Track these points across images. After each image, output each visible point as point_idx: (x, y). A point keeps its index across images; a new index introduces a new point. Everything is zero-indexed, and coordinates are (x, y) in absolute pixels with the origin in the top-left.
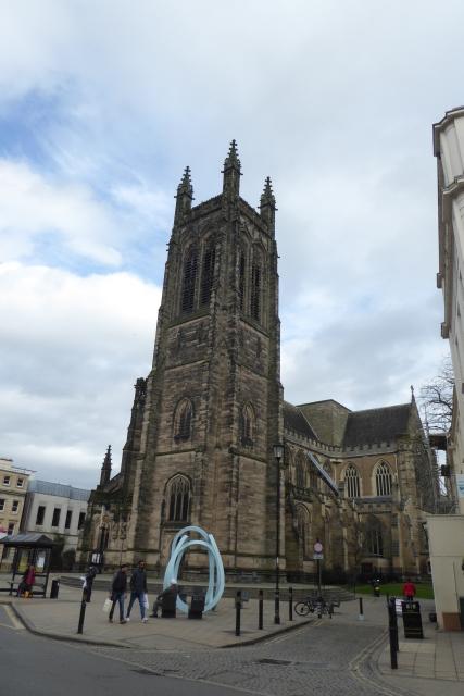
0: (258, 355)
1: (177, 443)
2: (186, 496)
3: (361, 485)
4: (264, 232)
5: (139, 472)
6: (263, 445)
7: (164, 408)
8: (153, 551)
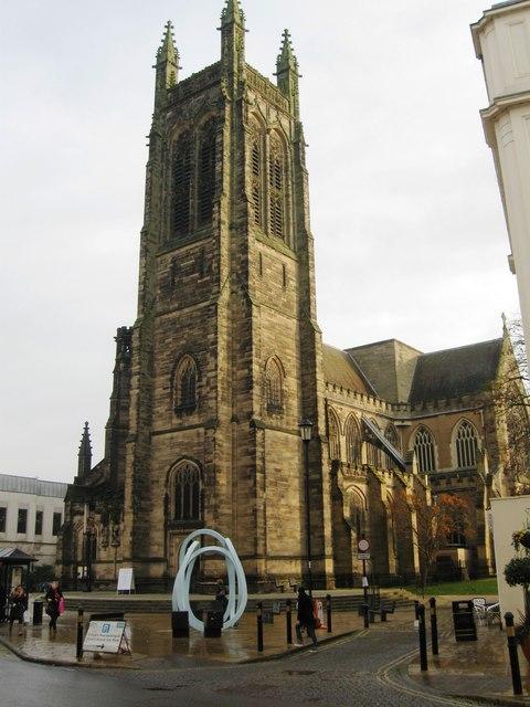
1: (179, 417)
2: (196, 486)
3: (436, 455)
5: (130, 458)
7: (158, 371)
8: (157, 560)
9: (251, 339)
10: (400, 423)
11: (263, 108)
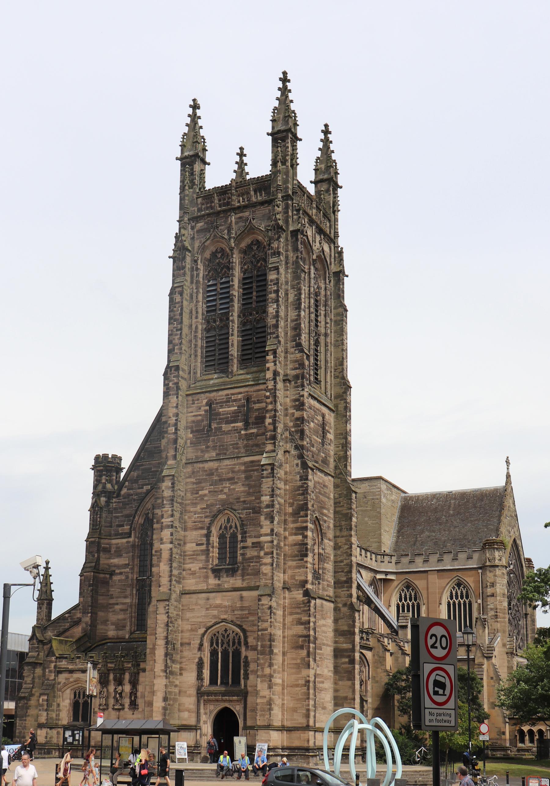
0: (323, 443)
2: (237, 654)
4: (325, 234)
6: (329, 577)
9: (306, 504)
10: (383, 576)
11: (309, 233)
